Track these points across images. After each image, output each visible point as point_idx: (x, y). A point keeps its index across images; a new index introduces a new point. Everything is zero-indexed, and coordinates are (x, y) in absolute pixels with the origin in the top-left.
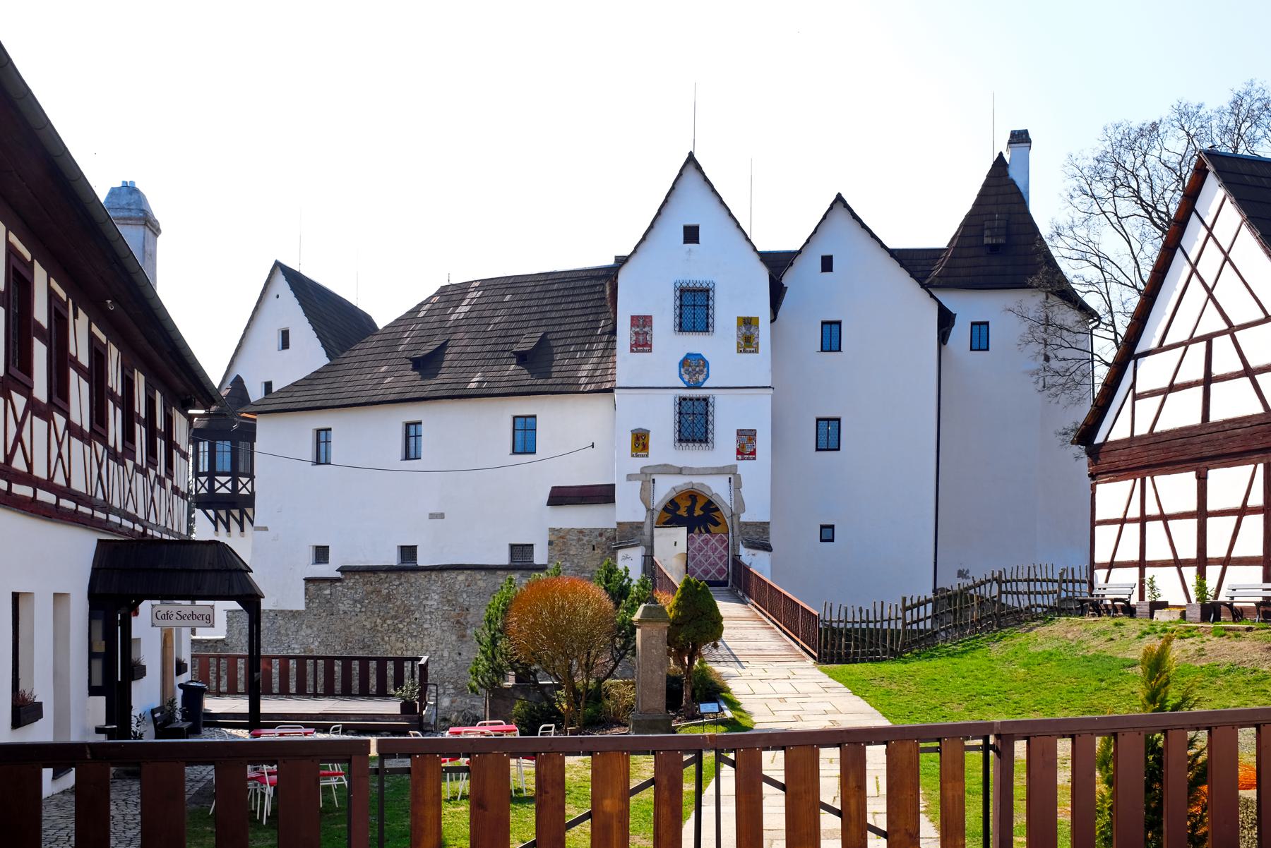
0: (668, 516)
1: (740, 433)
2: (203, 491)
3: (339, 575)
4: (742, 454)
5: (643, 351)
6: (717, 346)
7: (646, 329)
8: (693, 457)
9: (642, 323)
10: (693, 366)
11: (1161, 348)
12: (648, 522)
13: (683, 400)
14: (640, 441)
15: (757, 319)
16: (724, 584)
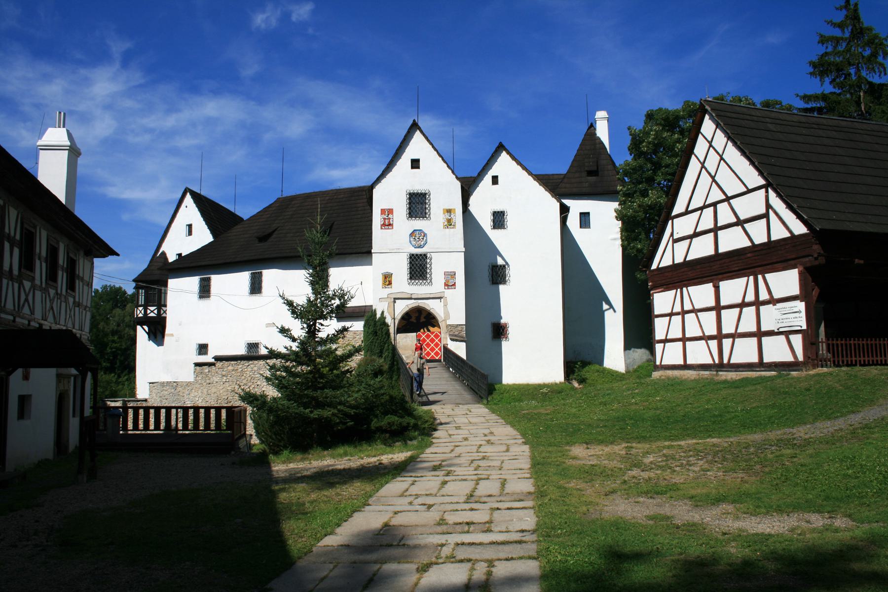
2: (141, 315)
3: (213, 360)
4: (448, 285)
6: (433, 225)
7: (390, 216)
8: (420, 289)
10: (417, 236)
11: (687, 212)
14: (387, 279)
16: (439, 361)
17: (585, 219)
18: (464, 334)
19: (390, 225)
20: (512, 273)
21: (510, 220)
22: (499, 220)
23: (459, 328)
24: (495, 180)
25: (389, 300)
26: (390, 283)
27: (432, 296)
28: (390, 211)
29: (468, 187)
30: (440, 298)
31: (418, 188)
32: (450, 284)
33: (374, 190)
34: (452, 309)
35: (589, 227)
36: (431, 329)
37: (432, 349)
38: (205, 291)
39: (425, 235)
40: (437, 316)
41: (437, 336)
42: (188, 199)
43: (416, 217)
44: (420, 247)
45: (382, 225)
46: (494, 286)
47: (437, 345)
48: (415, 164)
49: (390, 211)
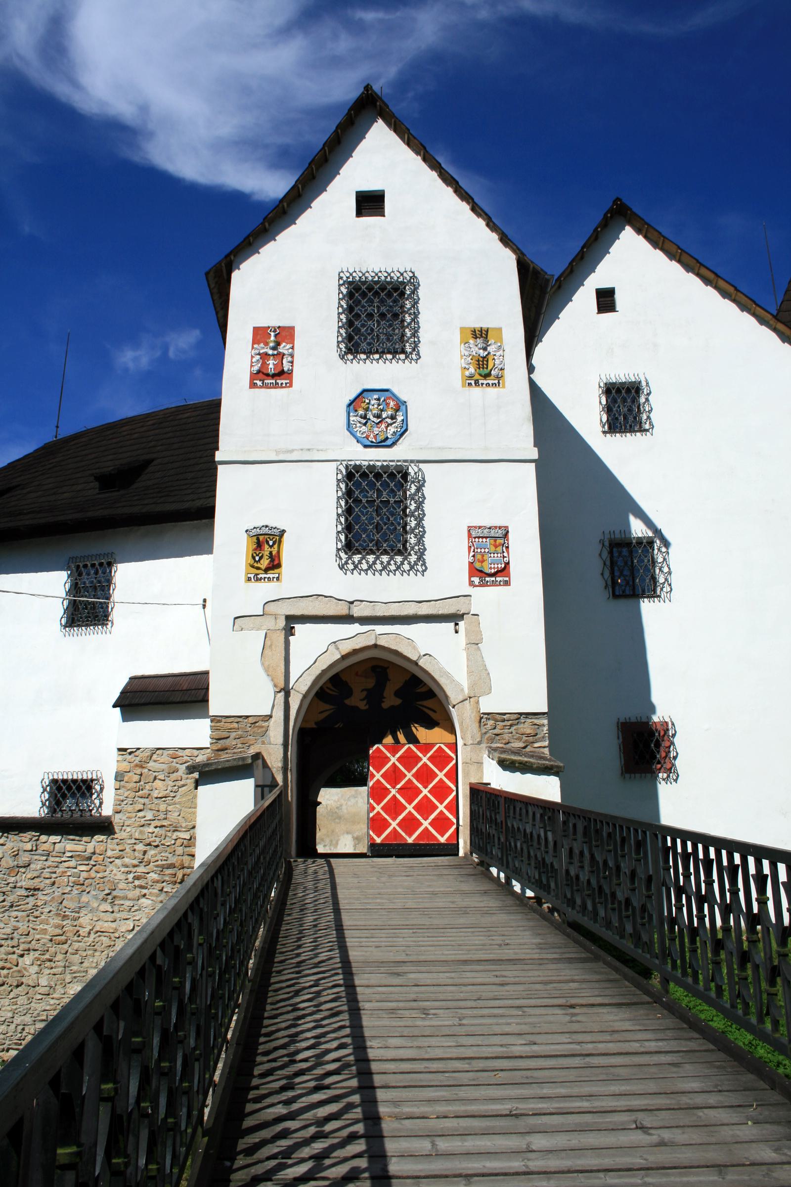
0: (326, 709)
1: (474, 534)
4: (481, 573)
5: (276, 386)
6: (426, 380)
7: (284, 348)
8: (381, 586)
10: (377, 412)
12: (279, 715)
14: (266, 551)
15: (500, 330)
16: (451, 849)
18: (543, 746)
19: (281, 374)
20: (680, 564)
21: (659, 406)
22: (625, 406)
23: (526, 727)
24: (606, 300)
25: (269, 623)
26: (275, 564)
27: (424, 610)
28: (285, 334)
30: (455, 618)
32: (490, 569)
33: (236, 276)
34: (496, 658)
36: (422, 734)
37: (425, 808)
39: (400, 405)
40: (442, 681)
41: (441, 759)
43: (369, 353)
44: (382, 443)
45: (254, 376)
46: (623, 604)
47: (441, 791)
49: (285, 334)
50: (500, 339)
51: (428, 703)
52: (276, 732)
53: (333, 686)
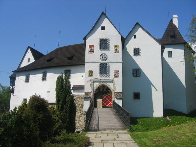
2: (11, 89)
9: (92, 47)
10: (104, 57)
13: (101, 64)
14: (91, 73)
15: (118, 46)
17: (170, 54)
18: (121, 96)
21: (142, 52)
25: (91, 81)
26: (92, 75)
28: (93, 46)
29: (124, 41)
31: (104, 37)
32: (116, 76)
35: (172, 57)
36: (108, 94)
38: (27, 80)
39: (106, 56)
40: (111, 88)
42: (29, 50)
44: (104, 60)
48: (103, 28)
49: (93, 46)
50: (119, 47)
51: (109, 90)
52: (92, 94)
53: (98, 88)
